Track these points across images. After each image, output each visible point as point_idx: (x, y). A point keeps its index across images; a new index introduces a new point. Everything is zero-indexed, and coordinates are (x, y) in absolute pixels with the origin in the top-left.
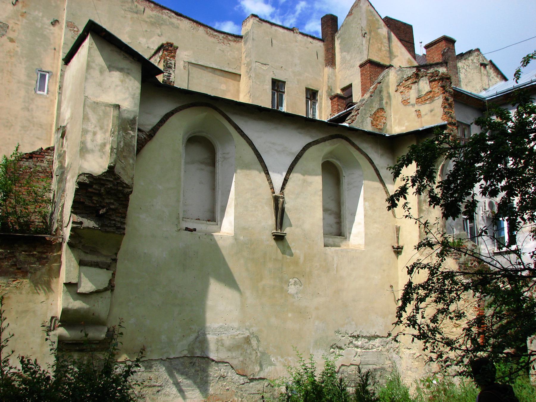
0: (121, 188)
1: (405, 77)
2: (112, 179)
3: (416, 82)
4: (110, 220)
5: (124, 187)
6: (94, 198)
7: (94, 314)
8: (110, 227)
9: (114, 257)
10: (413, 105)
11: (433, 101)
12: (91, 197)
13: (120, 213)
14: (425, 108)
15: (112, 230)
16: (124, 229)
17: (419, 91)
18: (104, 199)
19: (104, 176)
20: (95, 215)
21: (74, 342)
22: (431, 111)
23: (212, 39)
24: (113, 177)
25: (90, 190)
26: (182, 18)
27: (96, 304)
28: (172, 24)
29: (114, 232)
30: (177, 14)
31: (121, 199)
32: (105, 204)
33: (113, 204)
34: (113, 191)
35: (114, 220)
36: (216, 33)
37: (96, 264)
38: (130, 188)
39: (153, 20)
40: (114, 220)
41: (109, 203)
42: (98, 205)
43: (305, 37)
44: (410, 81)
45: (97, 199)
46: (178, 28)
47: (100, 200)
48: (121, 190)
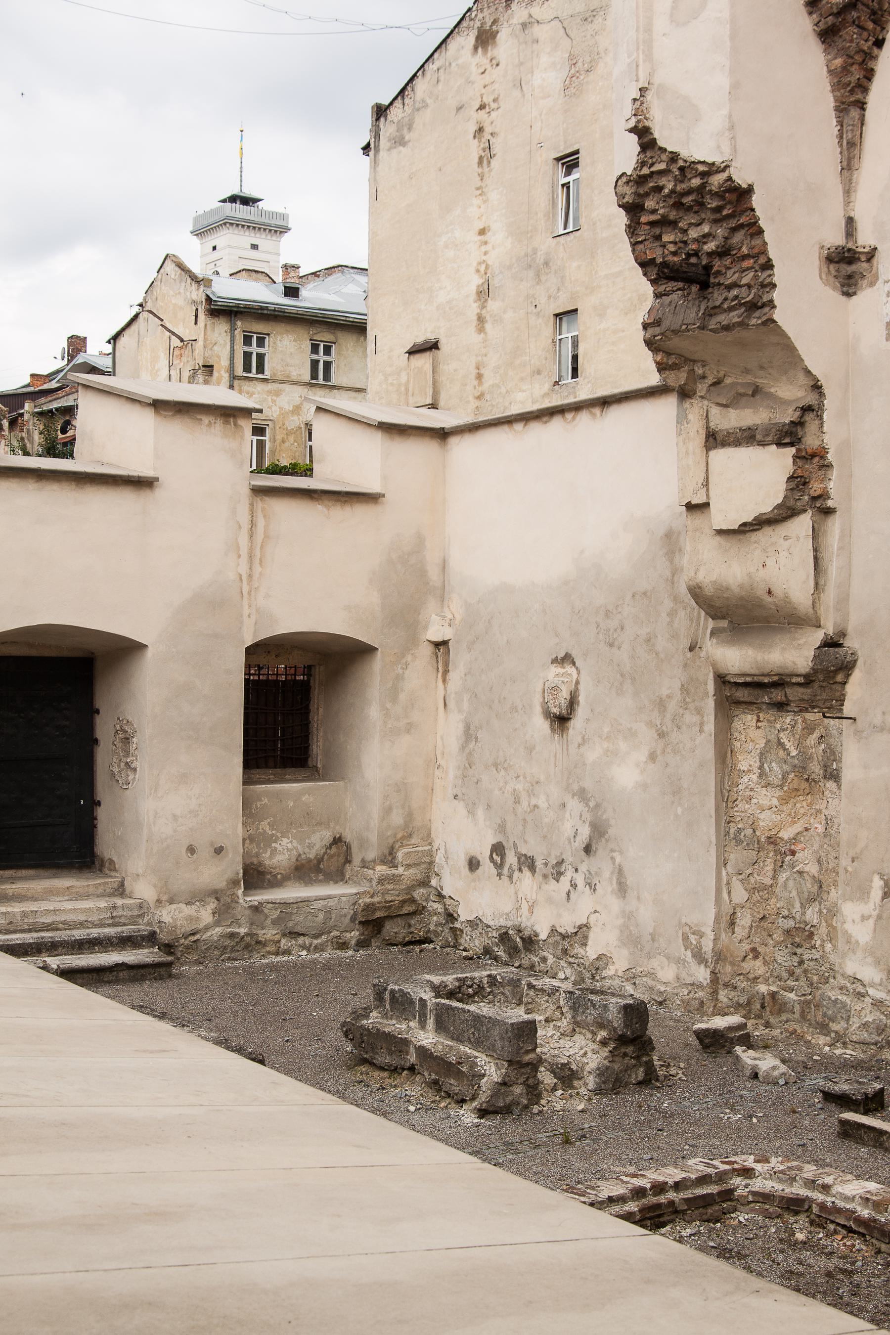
0: (696, 182)
2: (662, 166)
5: (703, 175)
6: (666, 238)
8: (731, 309)
9: (811, 399)
12: (658, 238)
13: (745, 257)
15: (736, 320)
16: (771, 304)
18: (685, 231)
19: (643, 164)
21: (749, 679)
27: (770, 563)
29: (742, 324)
31: (725, 212)
34: (687, 200)
35: (735, 285)
37: (746, 434)
38: (724, 170)
40: (735, 285)
48: (703, 186)
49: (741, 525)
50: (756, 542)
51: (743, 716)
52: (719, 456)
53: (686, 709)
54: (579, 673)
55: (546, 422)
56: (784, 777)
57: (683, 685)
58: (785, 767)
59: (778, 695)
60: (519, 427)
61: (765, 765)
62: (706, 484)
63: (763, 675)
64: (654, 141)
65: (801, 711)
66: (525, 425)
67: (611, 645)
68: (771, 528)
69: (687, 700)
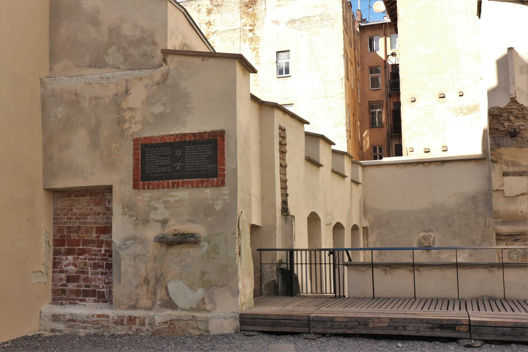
4: (522, 137)
6: (505, 124)
7: (522, 212)
12: (503, 124)
18: (513, 123)
19: (509, 106)
20: (509, 136)
24: (517, 105)
25: (500, 118)
27: (523, 205)
32: (516, 127)
33: (523, 125)
41: (519, 125)
42: (510, 129)
45: (508, 124)
47: (511, 124)
49: (516, 195)
50: (518, 200)
51: (501, 243)
52: (507, 179)
53: (484, 242)
54: (435, 235)
55: (415, 166)
56: (518, 258)
57: (482, 236)
58: (518, 255)
59: (516, 237)
60: (402, 166)
61: (511, 255)
62: (503, 185)
63: (515, 233)
64: (516, 101)
65: (524, 241)
66: (405, 166)
67: (449, 226)
68: (522, 196)
69: (484, 240)
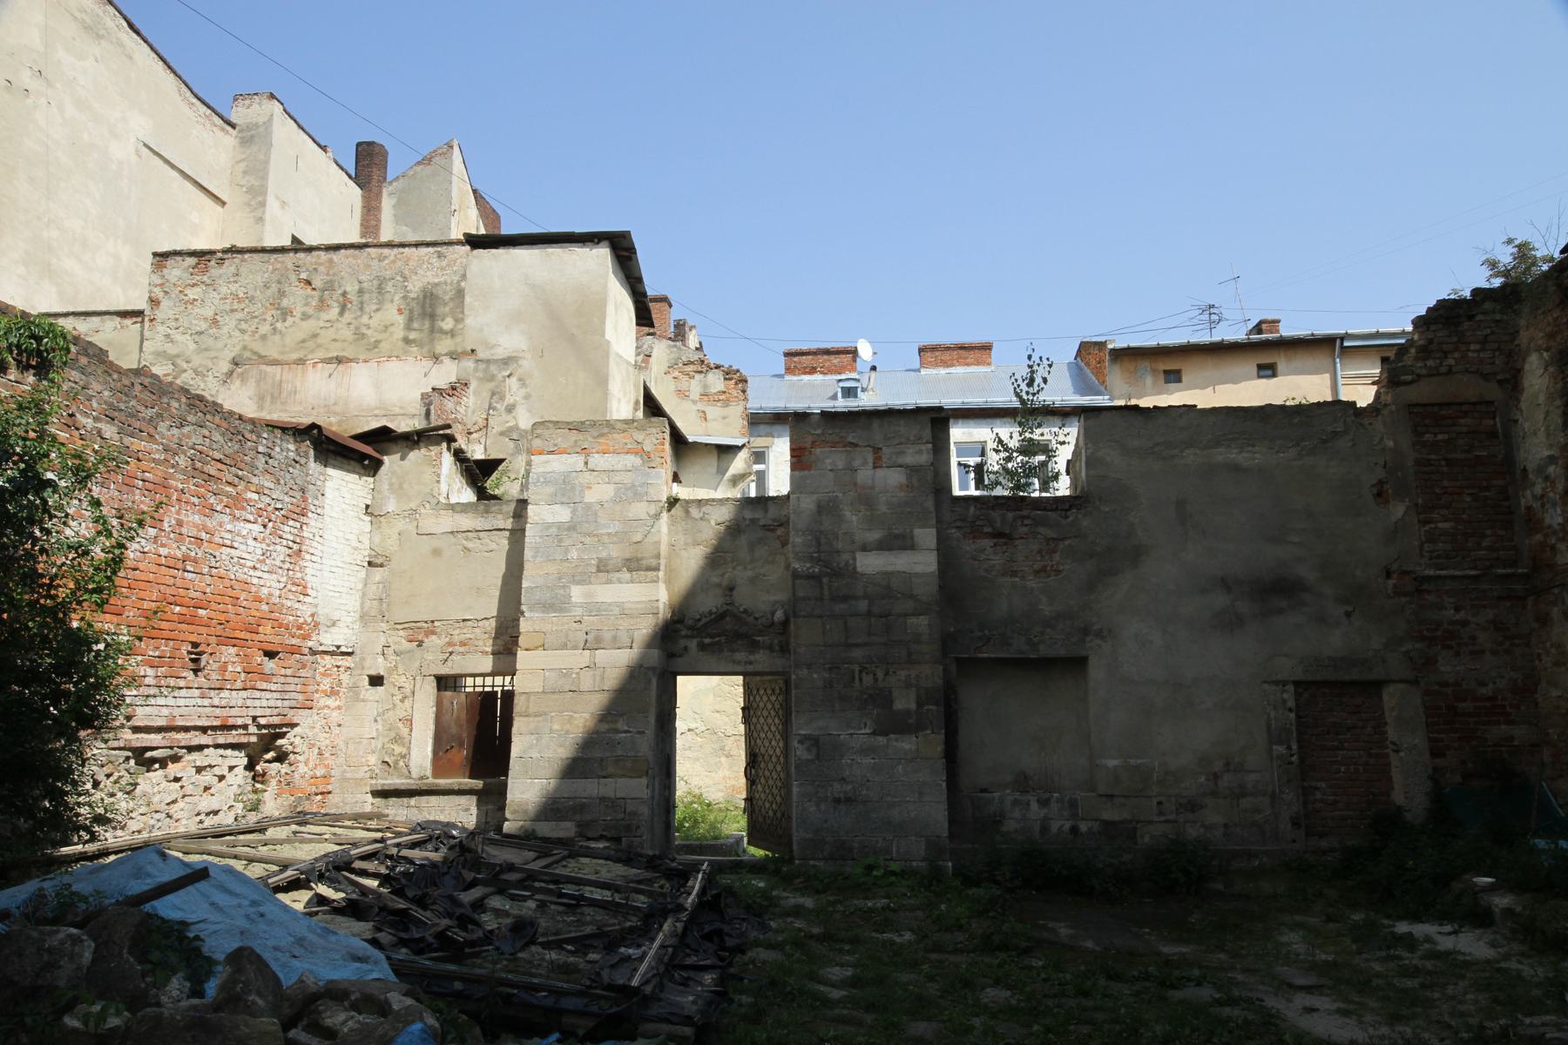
1: (684, 359)
3: (701, 372)
10: (694, 402)
11: (727, 406)
14: (714, 411)
17: (705, 386)
22: (724, 418)
23: (186, 109)
26: (138, 38)
28: (120, 44)
30: (131, 26)
36: (195, 100)
39: (87, 20)
43: (340, 171)
44: (690, 368)
46: (130, 58)
